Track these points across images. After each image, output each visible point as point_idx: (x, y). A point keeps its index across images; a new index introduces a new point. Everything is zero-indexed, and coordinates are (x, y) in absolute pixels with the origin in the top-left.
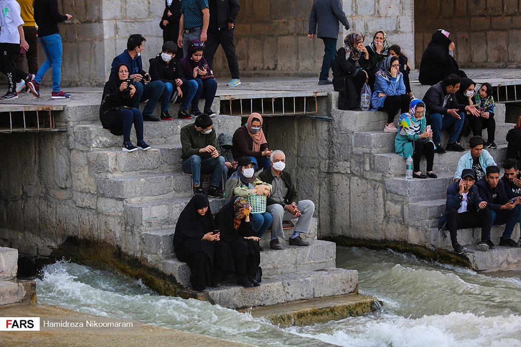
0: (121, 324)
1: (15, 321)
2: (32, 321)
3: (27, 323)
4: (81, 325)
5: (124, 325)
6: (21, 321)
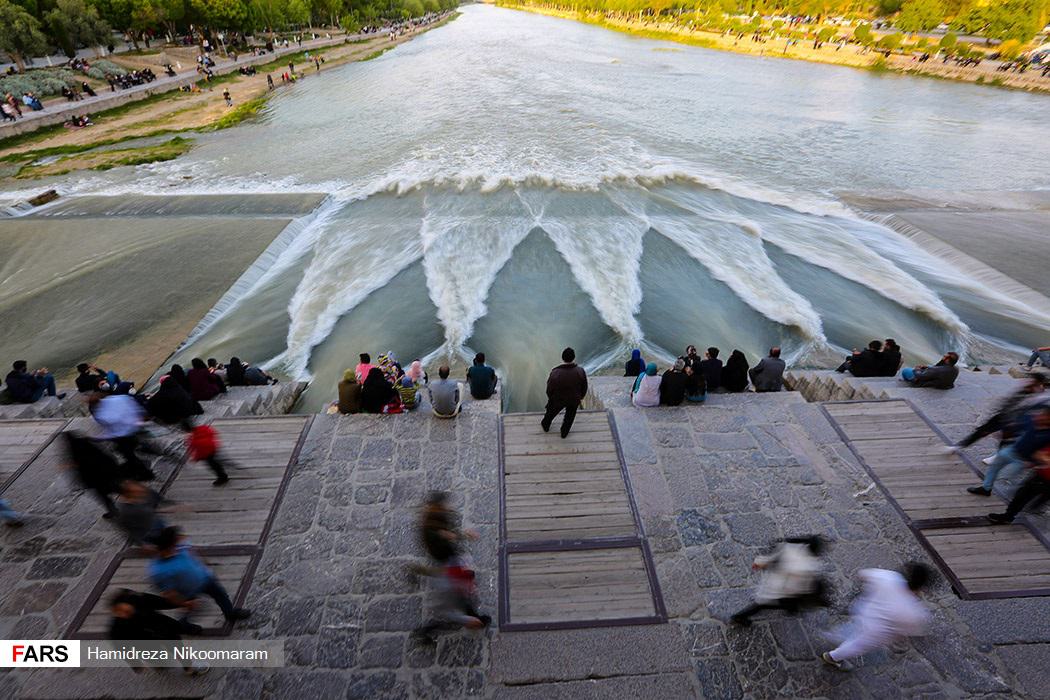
0: (244, 655)
1: (31, 648)
2: (65, 649)
3: (54, 651)
4: (164, 656)
5: (249, 657)
6: (42, 647)
